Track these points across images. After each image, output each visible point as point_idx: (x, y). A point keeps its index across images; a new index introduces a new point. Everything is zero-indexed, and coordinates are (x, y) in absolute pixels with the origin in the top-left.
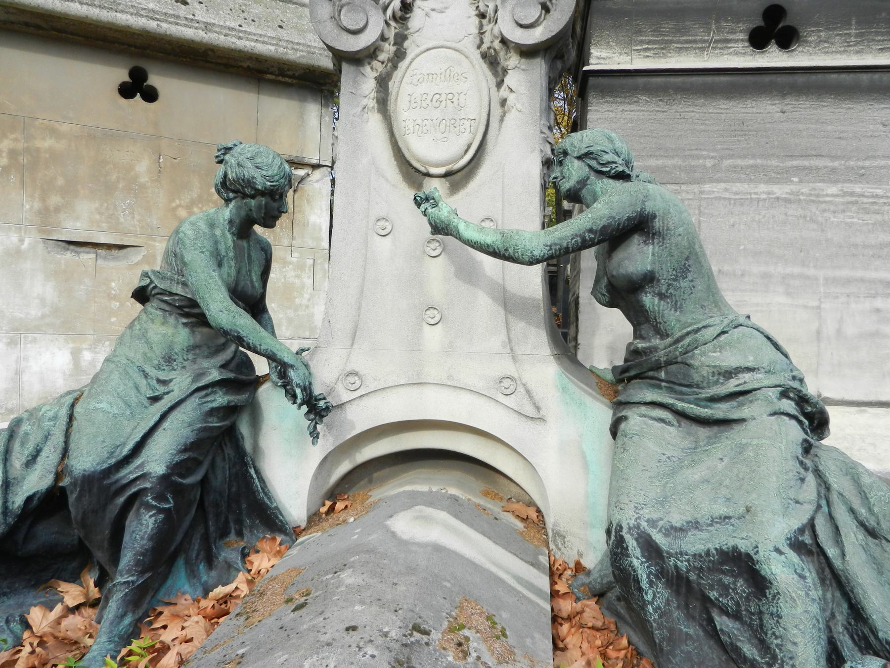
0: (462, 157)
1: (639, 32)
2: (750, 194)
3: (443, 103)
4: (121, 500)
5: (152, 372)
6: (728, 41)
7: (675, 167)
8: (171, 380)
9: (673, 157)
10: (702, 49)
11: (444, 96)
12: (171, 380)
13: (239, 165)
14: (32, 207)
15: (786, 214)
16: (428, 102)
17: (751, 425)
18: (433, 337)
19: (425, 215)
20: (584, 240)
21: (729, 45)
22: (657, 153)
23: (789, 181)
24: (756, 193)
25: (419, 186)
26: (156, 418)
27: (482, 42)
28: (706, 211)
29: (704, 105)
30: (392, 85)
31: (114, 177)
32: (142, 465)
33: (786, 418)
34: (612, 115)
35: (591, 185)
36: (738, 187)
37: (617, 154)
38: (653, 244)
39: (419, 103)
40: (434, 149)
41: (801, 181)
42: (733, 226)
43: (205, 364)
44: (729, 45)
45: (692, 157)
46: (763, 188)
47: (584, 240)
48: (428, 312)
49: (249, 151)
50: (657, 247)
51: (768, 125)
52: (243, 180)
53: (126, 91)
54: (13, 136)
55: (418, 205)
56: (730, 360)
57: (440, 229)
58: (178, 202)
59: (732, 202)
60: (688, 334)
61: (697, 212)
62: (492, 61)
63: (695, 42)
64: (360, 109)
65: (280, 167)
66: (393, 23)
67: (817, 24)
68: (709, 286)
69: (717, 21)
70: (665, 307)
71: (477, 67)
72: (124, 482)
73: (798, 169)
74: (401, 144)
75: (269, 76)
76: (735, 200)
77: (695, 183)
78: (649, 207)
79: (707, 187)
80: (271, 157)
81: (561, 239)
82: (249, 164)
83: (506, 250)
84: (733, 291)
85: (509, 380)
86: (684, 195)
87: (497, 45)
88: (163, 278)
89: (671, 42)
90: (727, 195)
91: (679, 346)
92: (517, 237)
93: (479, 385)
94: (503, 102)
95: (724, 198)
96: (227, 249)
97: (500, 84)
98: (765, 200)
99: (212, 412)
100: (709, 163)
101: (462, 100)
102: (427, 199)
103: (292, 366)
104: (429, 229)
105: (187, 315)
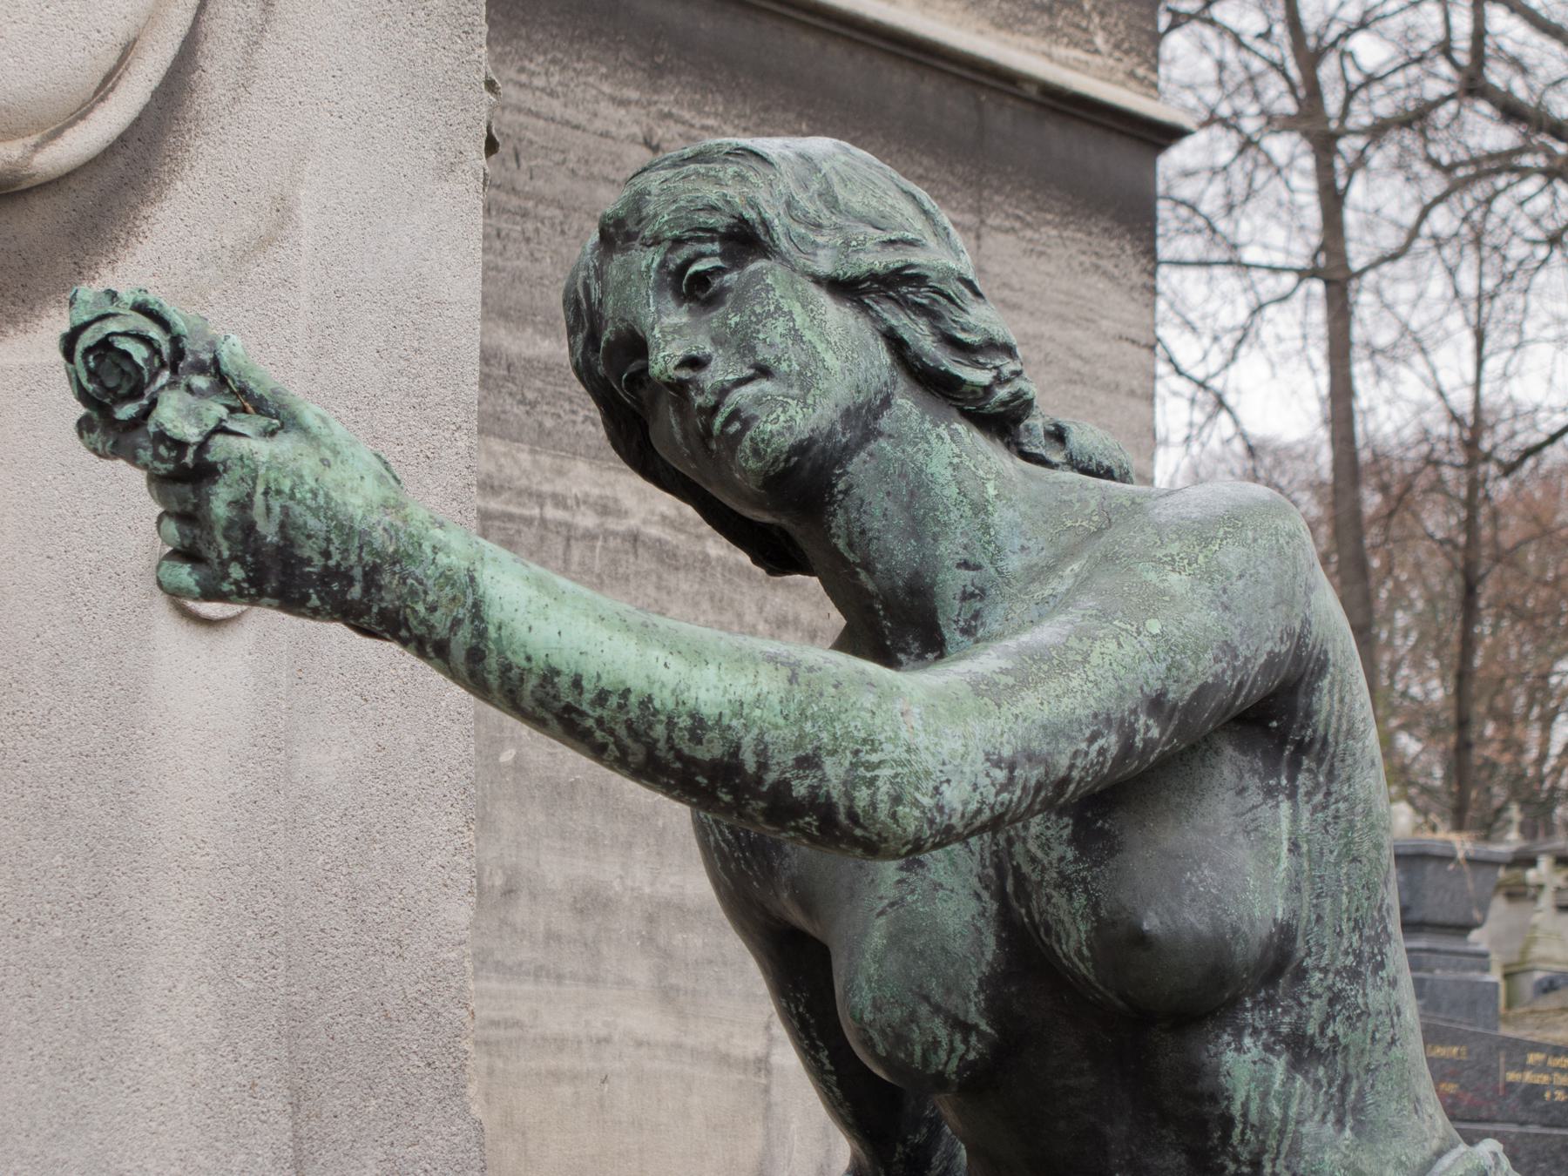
2: (540, 498)
24: (559, 501)
35: (897, 438)
38: (1292, 796)
50: (1306, 815)
70: (1308, 1104)
81: (1053, 732)
83: (808, 762)
98: (590, 536)
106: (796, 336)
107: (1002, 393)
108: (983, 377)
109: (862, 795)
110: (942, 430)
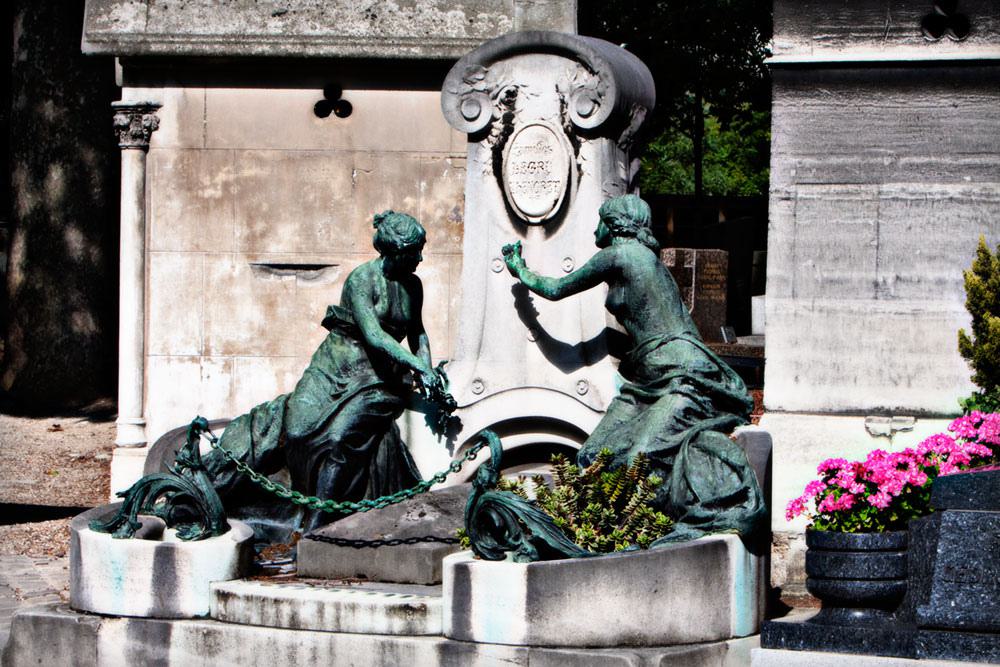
1: (819, 21)
2: (926, 194)
4: (315, 457)
5: (335, 379)
6: (902, 30)
7: (854, 165)
9: (852, 155)
10: (879, 39)
13: (387, 233)
14: (241, 234)
15: (959, 216)
17: (659, 402)
21: (904, 35)
22: (838, 151)
23: (961, 181)
24: (930, 194)
28: (884, 213)
29: (881, 99)
30: (504, 153)
31: (311, 197)
32: (327, 436)
34: (794, 109)
36: (913, 187)
40: (536, 203)
41: (973, 181)
42: (910, 228)
44: (904, 35)
45: (870, 154)
46: (937, 187)
51: (942, 120)
53: (321, 110)
54: (226, 169)
59: (909, 203)
61: (876, 213)
63: (871, 31)
66: (503, 107)
67: (985, 13)
69: (893, 8)
71: (560, 139)
72: (317, 445)
73: (970, 167)
76: (912, 200)
77: (873, 183)
78: (618, 262)
79: (885, 187)
82: (392, 232)
84: (910, 299)
86: (864, 196)
89: (849, 31)
90: (904, 196)
94: (579, 167)
95: (902, 200)
96: (382, 289)
97: (577, 153)
98: (939, 201)
99: (372, 406)
100: (887, 161)
103: (422, 373)
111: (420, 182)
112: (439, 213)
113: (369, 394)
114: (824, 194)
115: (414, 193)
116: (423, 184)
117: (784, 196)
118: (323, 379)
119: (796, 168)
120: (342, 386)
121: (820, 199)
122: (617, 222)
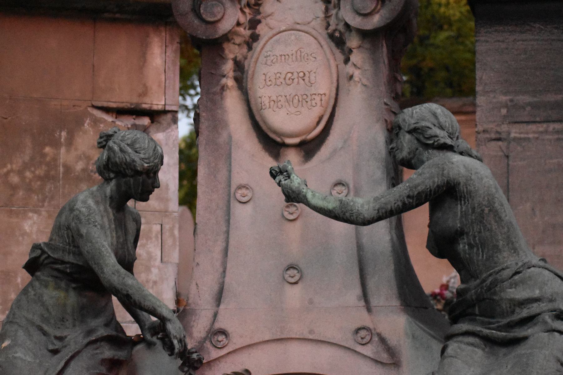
0: (315, 128)
3: (296, 80)
8: (66, 337)
11: (295, 75)
12: (66, 337)
13: (121, 150)
16: (282, 80)
18: (294, 295)
19: (280, 186)
20: (404, 204)
25: (276, 156)
26: (62, 364)
27: (328, 25)
33: (556, 334)
34: (503, 46)
37: (442, 128)
39: (274, 81)
40: (290, 121)
43: (94, 323)
47: (404, 204)
48: (289, 272)
49: (128, 138)
52: (125, 164)
55: (274, 176)
56: (520, 294)
57: (293, 197)
58: (9, 166)
60: (491, 275)
62: (338, 41)
64: (219, 88)
65: (154, 150)
66: (247, 10)
68: (508, 237)
71: (325, 47)
74: (258, 118)
75: (106, 15)
80: (147, 142)
81: (386, 204)
82: (130, 150)
85: (365, 331)
87: (341, 27)
88: (55, 249)
91: (484, 284)
92: (352, 203)
93: (338, 338)
97: (347, 61)
101: (312, 78)
102: (281, 172)
103: (169, 320)
104: (284, 197)
105: (74, 281)
106: (401, 142)
107: (436, 143)
108: (431, 142)
109: (352, 218)
110: (426, 152)
111: (61, 132)
112: (80, 166)
113: (97, 349)
114: (542, 132)
115: (56, 144)
116: (64, 134)
117: (493, 136)
118: (32, 330)
119: (506, 106)
120: (61, 339)
121: (537, 138)
122: (430, 132)
